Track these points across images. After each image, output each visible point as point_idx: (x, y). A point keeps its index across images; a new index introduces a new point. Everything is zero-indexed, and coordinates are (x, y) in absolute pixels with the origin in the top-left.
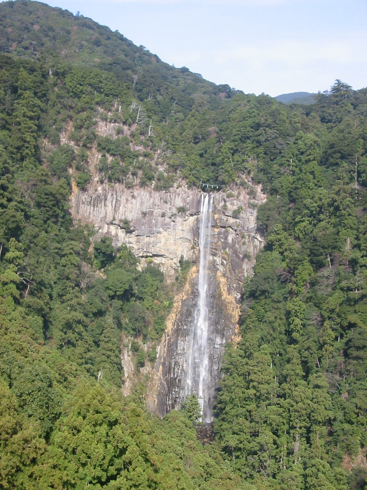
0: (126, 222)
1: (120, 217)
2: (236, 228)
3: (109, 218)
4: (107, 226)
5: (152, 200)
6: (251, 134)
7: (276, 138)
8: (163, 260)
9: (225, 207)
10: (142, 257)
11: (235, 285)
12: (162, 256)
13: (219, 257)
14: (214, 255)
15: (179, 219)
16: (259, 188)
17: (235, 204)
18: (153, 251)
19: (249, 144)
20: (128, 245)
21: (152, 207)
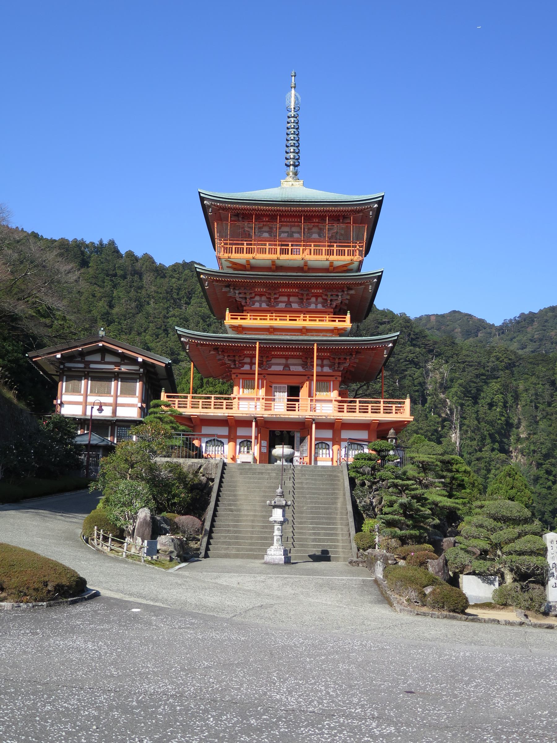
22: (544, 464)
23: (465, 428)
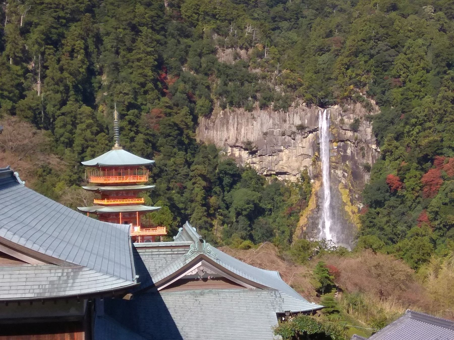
0: (249, 143)
1: (242, 140)
2: (354, 141)
3: (232, 141)
4: (230, 148)
5: (271, 121)
6: (364, 47)
7: (387, 50)
8: (286, 177)
9: (342, 121)
10: (267, 175)
11: (357, 196)
12: (285, 173)
13: (341, 170)
14: (336, 168)
15: (298, 137)
16: (373, 102)
17: (352, 117)
18: (277, 169)
19: (361, 59)
20: (252, 165)
21: (271, 127)
22: (127, 115)
23: (47, 80)
